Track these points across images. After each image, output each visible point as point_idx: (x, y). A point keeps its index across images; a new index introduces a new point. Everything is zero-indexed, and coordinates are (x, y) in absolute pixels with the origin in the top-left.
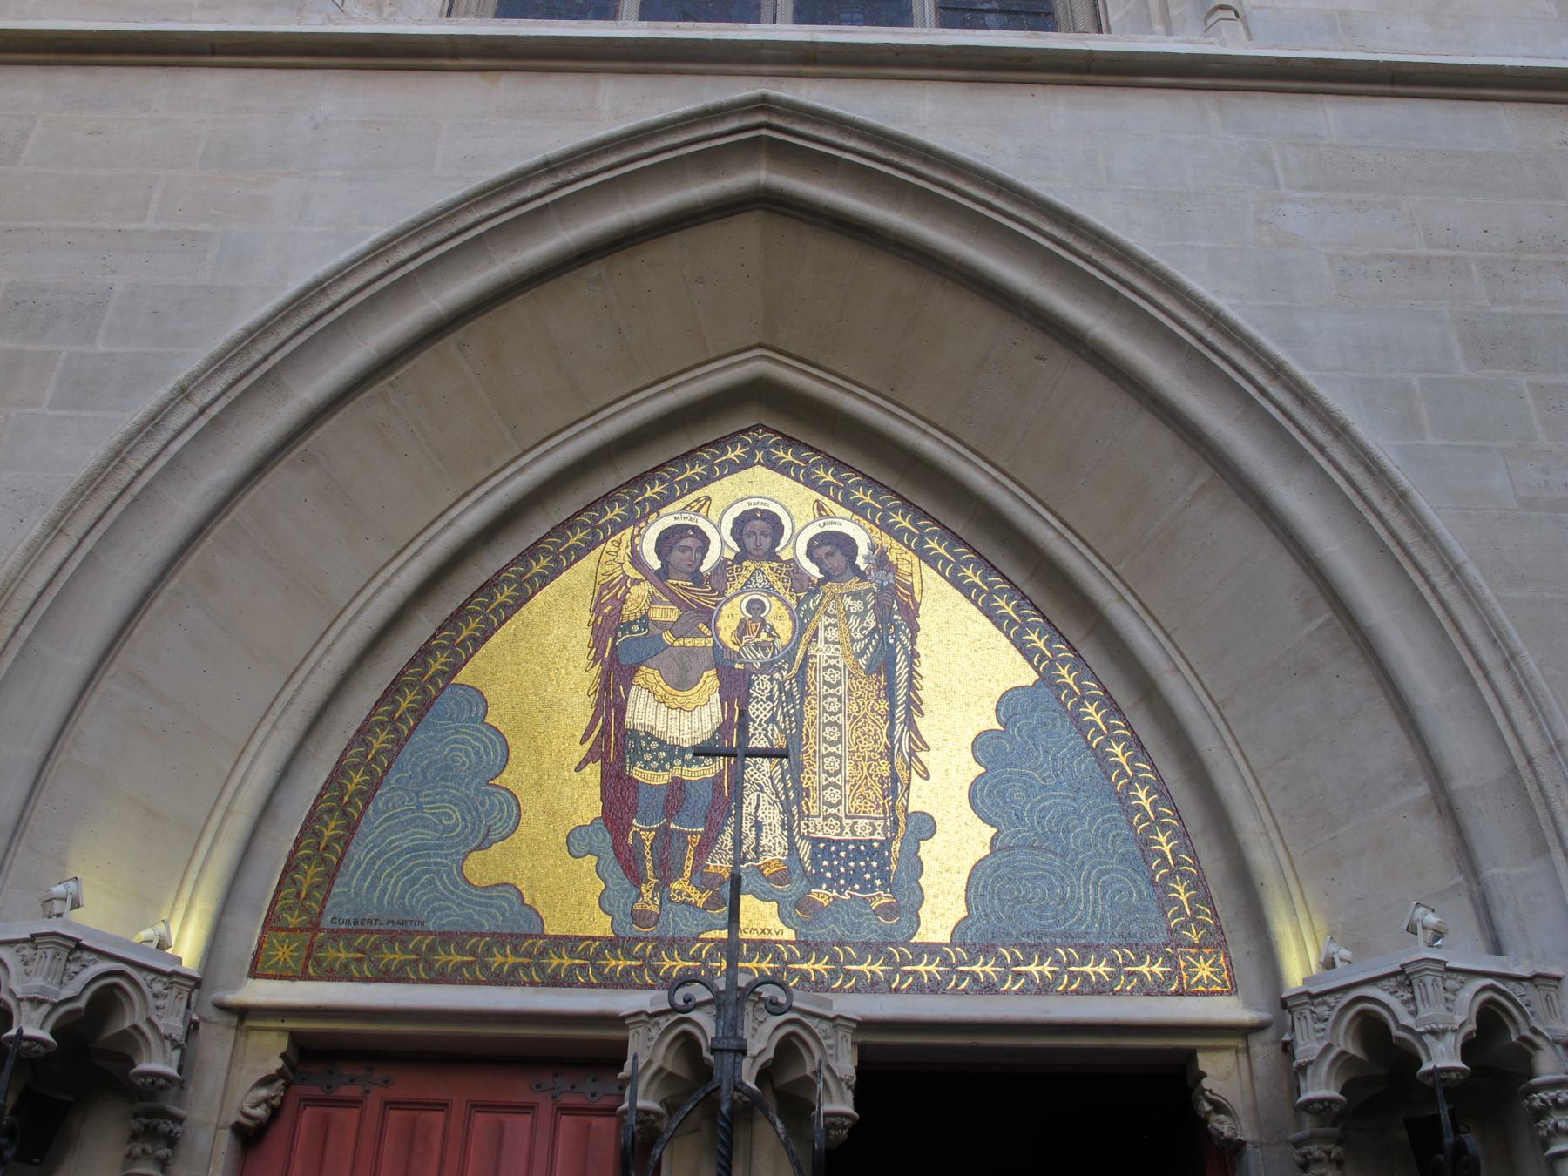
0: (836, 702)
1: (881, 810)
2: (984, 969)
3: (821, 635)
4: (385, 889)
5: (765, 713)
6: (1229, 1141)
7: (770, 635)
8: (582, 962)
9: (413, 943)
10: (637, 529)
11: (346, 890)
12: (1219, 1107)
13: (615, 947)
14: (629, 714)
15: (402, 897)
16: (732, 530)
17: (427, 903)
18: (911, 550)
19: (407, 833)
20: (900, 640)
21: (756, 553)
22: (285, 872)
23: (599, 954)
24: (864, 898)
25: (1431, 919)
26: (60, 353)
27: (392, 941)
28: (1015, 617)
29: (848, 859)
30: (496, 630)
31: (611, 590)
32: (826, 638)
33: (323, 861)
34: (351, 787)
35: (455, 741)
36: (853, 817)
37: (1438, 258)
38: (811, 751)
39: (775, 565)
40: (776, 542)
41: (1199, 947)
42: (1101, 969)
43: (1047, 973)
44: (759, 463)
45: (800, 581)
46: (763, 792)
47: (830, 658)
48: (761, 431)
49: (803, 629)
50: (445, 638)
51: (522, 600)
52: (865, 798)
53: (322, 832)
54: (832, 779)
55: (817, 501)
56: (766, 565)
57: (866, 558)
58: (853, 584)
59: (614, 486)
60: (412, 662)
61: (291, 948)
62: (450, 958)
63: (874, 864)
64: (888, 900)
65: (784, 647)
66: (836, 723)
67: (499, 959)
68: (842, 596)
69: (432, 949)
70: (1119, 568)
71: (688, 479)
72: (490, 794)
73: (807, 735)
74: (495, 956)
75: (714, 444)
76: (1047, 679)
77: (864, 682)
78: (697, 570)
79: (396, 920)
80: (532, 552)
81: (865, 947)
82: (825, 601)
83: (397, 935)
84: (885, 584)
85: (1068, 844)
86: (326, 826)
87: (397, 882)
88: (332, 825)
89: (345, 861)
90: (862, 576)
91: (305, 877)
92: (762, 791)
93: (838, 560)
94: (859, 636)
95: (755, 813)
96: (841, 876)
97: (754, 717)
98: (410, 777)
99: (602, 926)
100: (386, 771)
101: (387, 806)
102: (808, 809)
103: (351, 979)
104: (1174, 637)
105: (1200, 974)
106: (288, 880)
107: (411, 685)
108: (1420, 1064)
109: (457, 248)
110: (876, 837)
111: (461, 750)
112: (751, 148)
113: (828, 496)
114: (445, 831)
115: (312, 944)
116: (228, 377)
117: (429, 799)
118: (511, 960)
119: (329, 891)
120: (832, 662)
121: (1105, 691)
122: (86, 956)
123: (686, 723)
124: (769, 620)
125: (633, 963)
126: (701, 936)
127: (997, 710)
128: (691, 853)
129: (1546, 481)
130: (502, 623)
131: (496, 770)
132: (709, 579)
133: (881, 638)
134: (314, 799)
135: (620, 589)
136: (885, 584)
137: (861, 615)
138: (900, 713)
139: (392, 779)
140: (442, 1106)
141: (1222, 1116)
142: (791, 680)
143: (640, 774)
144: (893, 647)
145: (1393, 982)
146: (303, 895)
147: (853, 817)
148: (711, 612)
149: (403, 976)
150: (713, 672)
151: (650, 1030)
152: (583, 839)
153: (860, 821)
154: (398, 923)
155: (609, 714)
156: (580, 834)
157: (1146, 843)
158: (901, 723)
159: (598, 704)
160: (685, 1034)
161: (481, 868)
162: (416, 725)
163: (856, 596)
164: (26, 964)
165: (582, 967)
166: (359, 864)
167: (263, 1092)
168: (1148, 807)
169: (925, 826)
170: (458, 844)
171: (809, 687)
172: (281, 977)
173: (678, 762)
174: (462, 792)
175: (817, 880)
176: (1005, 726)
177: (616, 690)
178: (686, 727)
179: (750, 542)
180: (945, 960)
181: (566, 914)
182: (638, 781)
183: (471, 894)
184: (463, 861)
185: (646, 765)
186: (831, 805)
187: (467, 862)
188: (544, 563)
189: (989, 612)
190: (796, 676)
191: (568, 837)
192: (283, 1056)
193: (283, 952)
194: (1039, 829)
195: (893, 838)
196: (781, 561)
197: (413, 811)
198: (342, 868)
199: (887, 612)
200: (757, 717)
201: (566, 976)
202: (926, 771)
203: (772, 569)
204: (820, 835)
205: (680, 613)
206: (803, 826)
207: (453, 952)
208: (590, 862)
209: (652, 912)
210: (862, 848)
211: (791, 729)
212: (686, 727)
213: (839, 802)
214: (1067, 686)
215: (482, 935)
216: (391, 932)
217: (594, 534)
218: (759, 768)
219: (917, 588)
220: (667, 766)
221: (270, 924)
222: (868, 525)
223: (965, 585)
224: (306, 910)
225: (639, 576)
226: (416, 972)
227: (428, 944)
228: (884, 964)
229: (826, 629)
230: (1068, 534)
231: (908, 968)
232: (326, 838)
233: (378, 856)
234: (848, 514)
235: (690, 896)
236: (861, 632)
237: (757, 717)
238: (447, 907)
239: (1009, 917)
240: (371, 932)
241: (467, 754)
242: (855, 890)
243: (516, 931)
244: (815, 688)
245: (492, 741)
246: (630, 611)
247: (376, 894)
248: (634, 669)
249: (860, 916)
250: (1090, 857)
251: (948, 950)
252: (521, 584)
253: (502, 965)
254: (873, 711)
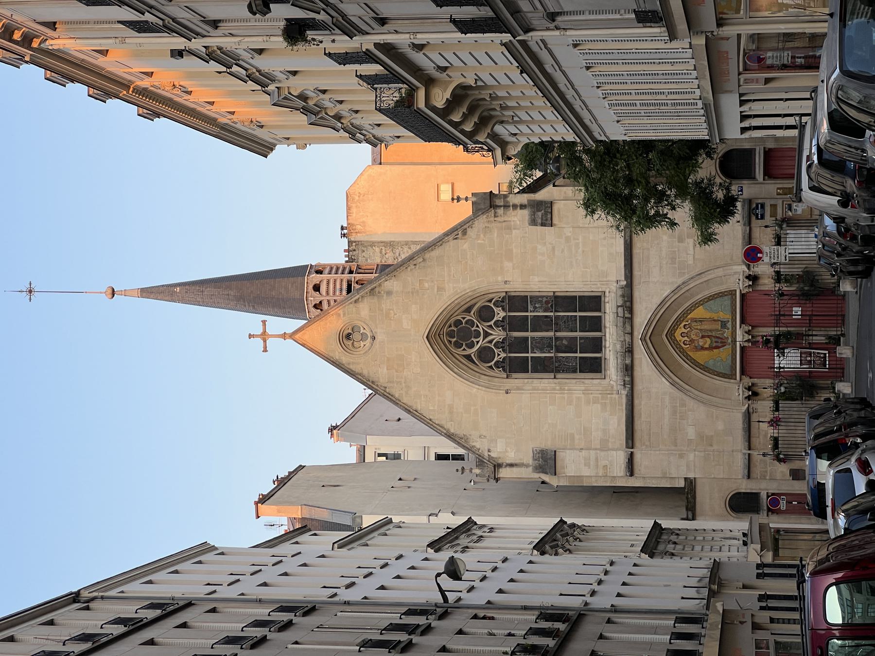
76: (702, 305)
83: (732, 367)
189: (694, 310)
193: (734, 377)
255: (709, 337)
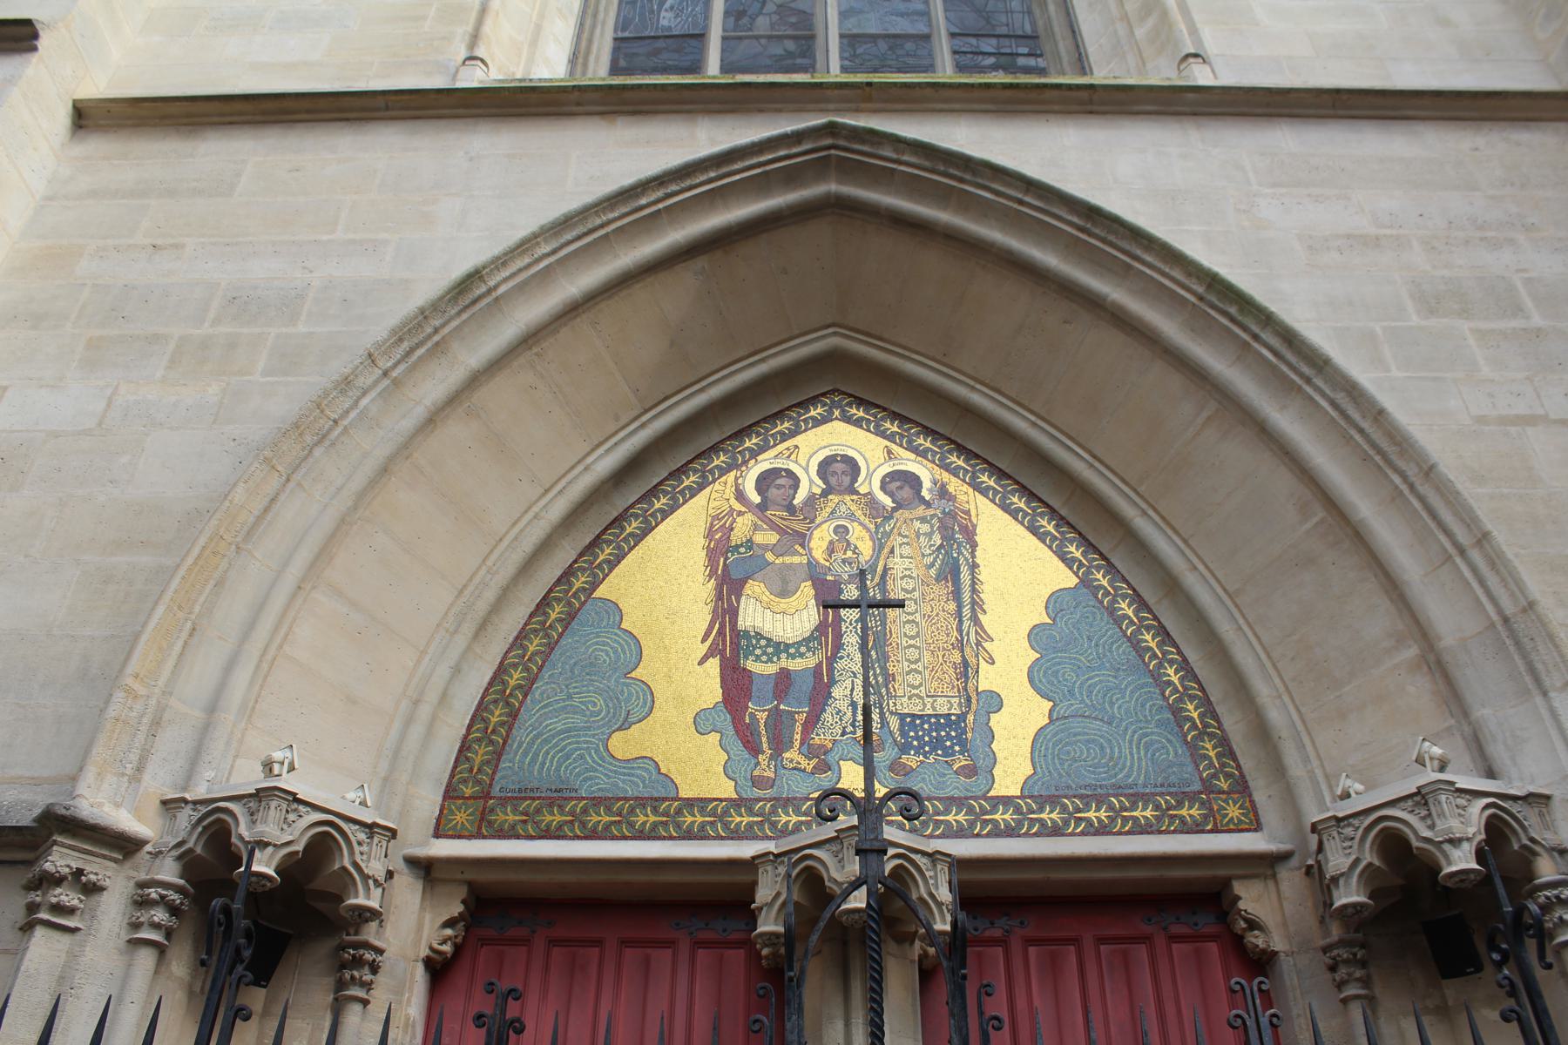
0: (913, 604)
1: (956, 690)
2: (1051, 816)
3: (897, 551)
4: (543, 764)
5: (854, 614)
6: (1264, 951)
7: (854, 553)
8: (712, 819)
9: (569, 807)
10: (739, 472)
11: (511, 765)
12: (1253, 925)
13: (739, 806)
14: (740, 618)
15: (558, 769)
16: (818, 471)
17: (578, 775)
18: (967, 483)
19: (560, 718)
20: (962, 554)
21: (838, 488)
22: (460, 751)
23: (726, 812)
24: (946, 761)
25: (1437, 751)
26: (269, 333)
27: (551, 806)
28: (1056, 534)
29: (930, 730)
30: (626, 554)
31: (720, 520)
32: (901, 554)
33: (491, 742)
34: (512, 683)
35: (597, 643)
36: (933, 696)
37: (1385, 236)
38: (894, 644)
39: (855, 497)
40: (855, 480)
41: (1228, 793)
42: (1148, 813)
43: (1103, 818)
44: (836, 418)
45: (877, 510)
46: (855, 677)
47: (906, 569)
48: (836, 394)
49: (881, 547)
50: (584, 562)
51: (647, 530)
52: (942, 680)
53: (489, 719)
54: (913, 666)
55: (886, 447)
56: (847, 498)
57: (930, 490)
58: (921, 511)
59: (719, 439)
60: (559, 581)
61: (468, 812)
62: (600, 818)
63: (953, 734)
64: (967, 763)
65: (867, 562)
66: (913, 621)
67: (642, 818)
68: (912, 520)
69: (585, 811)
70: (1142, 489)
71: (779, 432)
72: (628, 685)
73: (890, 631)
74: (638, 816)
75: (798, 405)
76: (1086, 582)
77: (935, 588)
78: (791, 503)
79: (553, 788)
80: (653, 492)
81: (952, 802)
82: (898, 525)
83: (556, 800)
84: (947, 510)
85: (1113, 713)
86: (493, 714)
87: (554, 757)
88: (497, 713)
89: (510, 741)
90: (928, 504)
91: (477, 755)
92: (855, 677)
93: (906, 493)
94: (928, 552)
95: (851, 695)
96: (926, 744)
97: (845, 618)
98: (560, 673)
99: (727, 789)
100: (540, 669)
101: (543, 698)
102: (895, 691)
103: (518, 837)
104: (1190, 542)
105: (1230, 815)
106: (462, 759)
107: (559, 600)
108: (1441, 870)
109: (588, 245)
110: (953, 711)
111: (602, 651)
112: (820, 167)
113: (895, 443)
114: (591, 716)
115: (484, 809)
116: (405, 345)
117: (576, 690)
118: (652, 819)
119: (497, 766)
120: (907, 573)
121: (1134, 590)
122: (301, 808)
123: (789, 624)
124: (853, 540)
125: (755, 819)
126: (811, 796)
127: (1046, 608)
128: (799, 728)
129: (1492, 403)
130: (631, 549)
131: (632, 666)
132: (801, 510)
133: (947, 552)
134: (482, 691)
135: (728, 520)
136: (947, 510)
137: (930, 535)
138: (966, 611)
139: (546, 674)
140: (598, 943)
141: (1256, 932)
142: (874, 587)
143: (752, 665)
144: (957, 560)
145: (1410, 803)
146: (475, 771)
147: (933, 696)
148: (805, 535)
149: (562, 834)
150: (809, 583)
151: (776, 868)
152: (708, 720)
153: (939, 699)
154: (556, 791)
155: (724, 618)
156: (705, 716)
157: (1176, 711)
158: (967, 620)
159: (715, 611)
160: (808, 868)
161: (623, 745)
162: (564, 631)
163: (923, 520)
164: (252, 814)
165: (712, 823)
166: (520, 746)
167: (449, 932)
168: (1177, 682)
169: (994, 702)
170: (603, 726)
171: (889, 593)
172: (460, 837)
173: (784, 656)
174: (604, 684)
175: (905, 748)
176: (1054, 620)
177: (729, 599)
178: (789, 627)
179: (833, 481)
180: (1018, 810)
181: (697, 780)
182: (751, 671)
183: (615, 766)
184: (608, 740)
185: (758, 658)
186: (914, 687)
187: (610, 740)
188: (664, 501)
189: (1034, 530)
190: (878, 584)
191: (695, 718)
192: (463, 902)
193: (461, 817)
194: (1088, 701)
195: (967, 712)
196: (860, 494)
197: (564, 700)
198: (507, 748)
199: (950, 532)
200: (848, 618)
201: (699, 831)
202: (991, 657)
203: (853, 501)
204: (906, 711)
205: (778, 537)
206: (891, 704)
207: (602, 813)
208: (715, 737)
209: (768, 777)
210: (942, 721)
211: (877, 627)
212: (789, 627)
213: (921, 685)
214: (1101, 587)
215: (626, 799)
216: (550, 798)
217: (703, 477)
218: (852, 659)
219: (973, 513)
220: (775, 659)
221: (450, 794)
222: (930, 465)
223: (1012, 510)
224: (478, 782)
225: (743, 509)
226: (572, 830)
227: (581, 808)
228: (966, 814)
229: (900, 547)
230: (1097, 464)
231: (987, 817)
232: (492, 724)
233: (539, 735)
234: (913, 456)
235: (800, 764)
236: (929, 549)
237: (848, 618)
238: (596, 777)
239: (1068, 775)
240: (533, 799)
241: (607, 655)
242: (938, 755)
243: (656, 795)
244: (895, 594)
245: (629, 645)
246: (737, 536)
247: (537, 767)
248: (743, 582)
249: (945, 775)
250: (1131, 723)
251: (1019, 801)
252: (646, 518)
253: (644, 823)
254: (944, 611)
255: (821, 628)
